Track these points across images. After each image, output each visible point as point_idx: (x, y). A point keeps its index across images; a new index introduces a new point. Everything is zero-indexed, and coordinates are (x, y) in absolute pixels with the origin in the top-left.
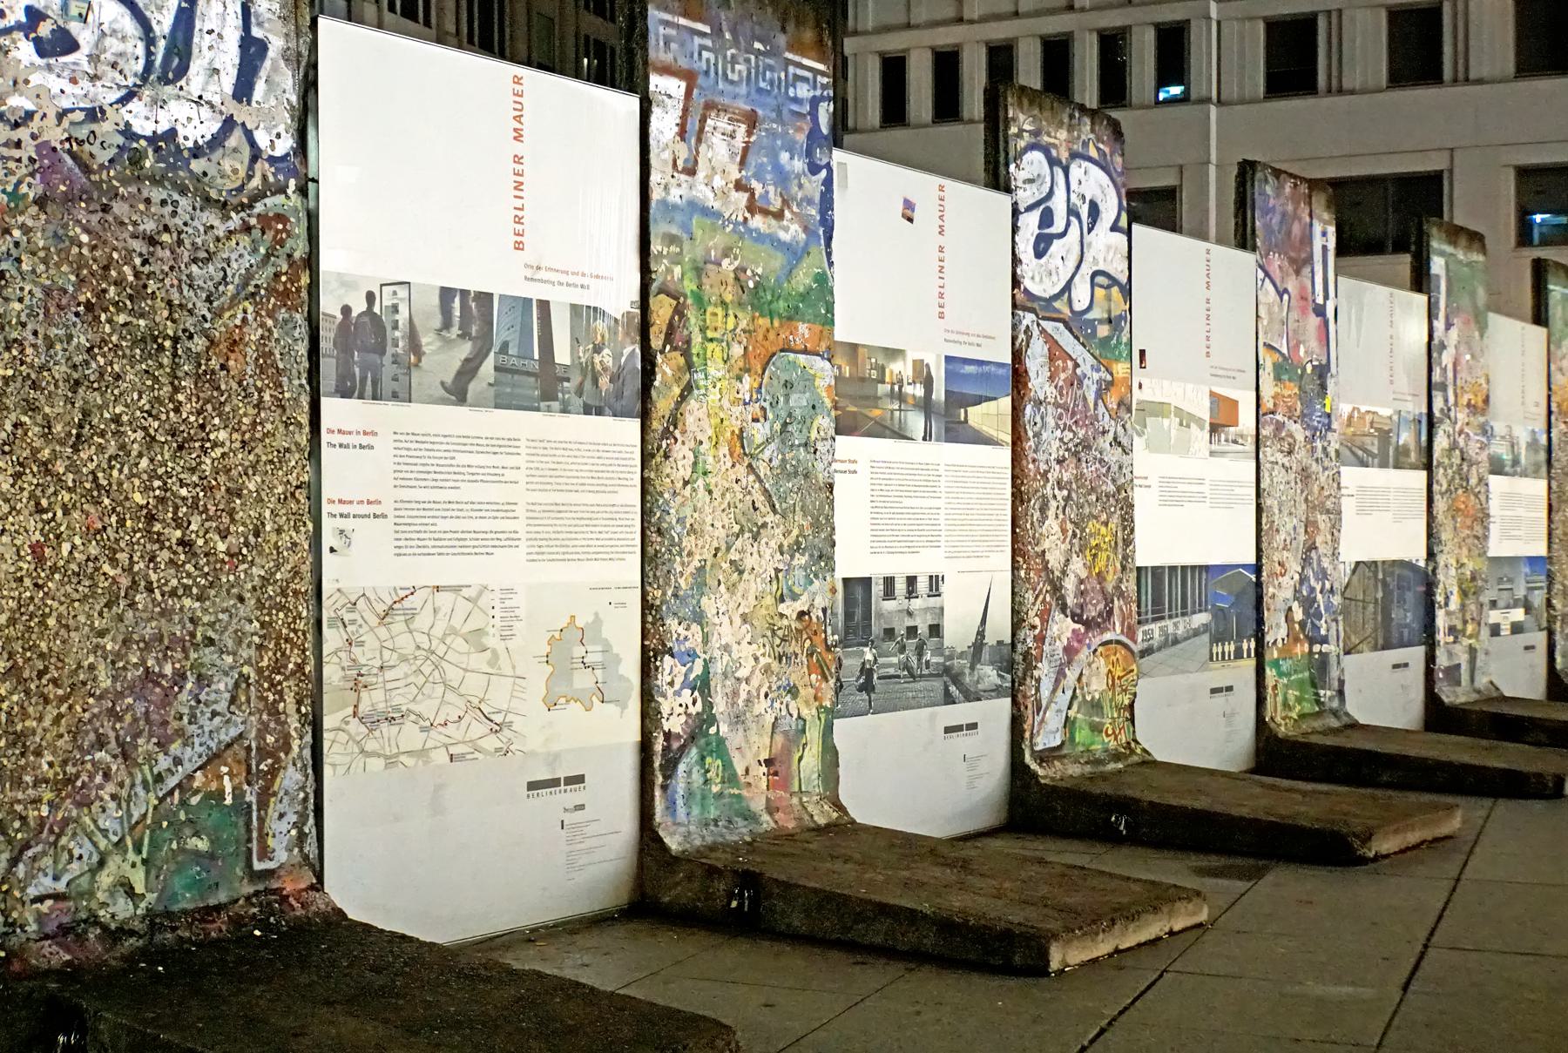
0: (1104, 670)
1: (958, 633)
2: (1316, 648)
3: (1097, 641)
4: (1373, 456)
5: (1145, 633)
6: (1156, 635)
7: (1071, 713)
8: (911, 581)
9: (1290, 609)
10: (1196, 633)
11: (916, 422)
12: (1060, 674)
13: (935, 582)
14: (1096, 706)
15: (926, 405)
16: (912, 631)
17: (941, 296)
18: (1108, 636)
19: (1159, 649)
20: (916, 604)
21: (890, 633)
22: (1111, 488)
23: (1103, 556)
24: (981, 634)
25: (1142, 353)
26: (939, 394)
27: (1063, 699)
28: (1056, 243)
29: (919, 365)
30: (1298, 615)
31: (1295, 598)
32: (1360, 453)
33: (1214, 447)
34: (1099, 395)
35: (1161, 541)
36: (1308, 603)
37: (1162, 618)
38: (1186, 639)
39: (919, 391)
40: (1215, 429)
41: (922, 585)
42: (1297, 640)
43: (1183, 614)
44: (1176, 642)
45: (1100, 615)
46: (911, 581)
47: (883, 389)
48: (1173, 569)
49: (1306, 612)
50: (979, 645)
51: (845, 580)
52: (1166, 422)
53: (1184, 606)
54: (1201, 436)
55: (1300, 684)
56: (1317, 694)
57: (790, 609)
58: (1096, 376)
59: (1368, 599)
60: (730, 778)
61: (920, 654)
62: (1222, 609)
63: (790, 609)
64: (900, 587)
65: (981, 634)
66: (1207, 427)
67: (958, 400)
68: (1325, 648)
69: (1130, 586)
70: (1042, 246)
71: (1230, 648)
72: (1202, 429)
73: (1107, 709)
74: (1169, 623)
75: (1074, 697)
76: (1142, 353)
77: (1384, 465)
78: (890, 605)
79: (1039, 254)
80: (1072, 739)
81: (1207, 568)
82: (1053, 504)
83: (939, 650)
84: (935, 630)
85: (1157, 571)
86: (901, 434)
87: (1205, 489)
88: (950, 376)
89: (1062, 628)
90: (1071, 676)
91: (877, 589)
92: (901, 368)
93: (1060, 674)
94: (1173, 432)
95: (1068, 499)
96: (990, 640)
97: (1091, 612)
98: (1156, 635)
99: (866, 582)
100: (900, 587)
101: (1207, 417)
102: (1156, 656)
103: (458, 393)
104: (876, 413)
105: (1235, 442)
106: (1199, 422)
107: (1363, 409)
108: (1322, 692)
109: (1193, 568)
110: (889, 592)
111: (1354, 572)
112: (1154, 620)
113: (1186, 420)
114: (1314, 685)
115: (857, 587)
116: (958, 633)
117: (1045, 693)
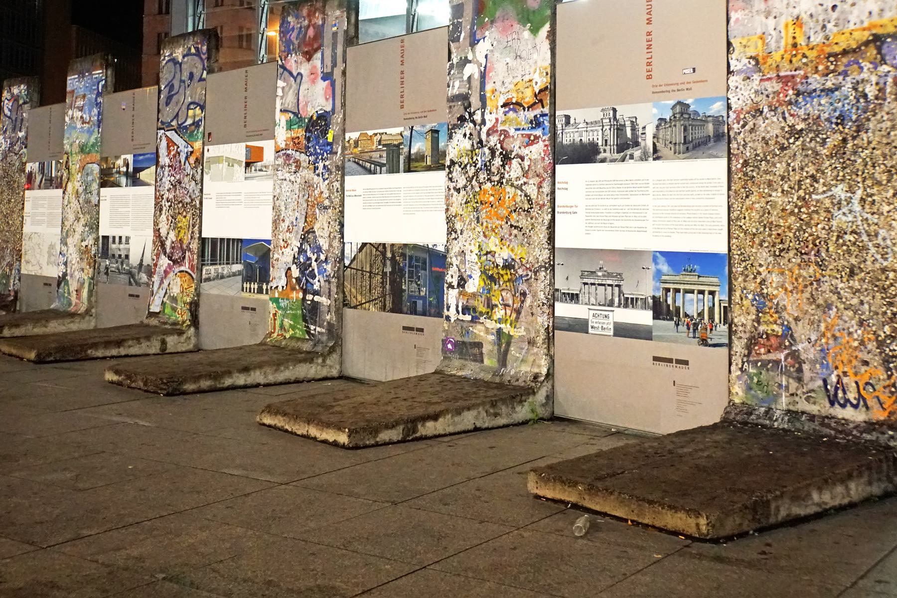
0: (179, 284)
1: (134, 260)
2: (309, 297)
3: (177, 270)
4: (381, 165)
5: (207, 270)
6: (213, 272)
7: (165, 300)
8: (120, 238)
9: (289, 269)
10: (234, 275)
11: (123, 180)
12: (162, 282)
13: (128, 239)
14: (174, 299)
15: (127, 174)
16: (120, 256)
17: (402, 97)
18: (182, 268)
19: (214, 279)
20: (122, 246)
21: (114, 255)
22: (189, 200)
23: (182, 231)
24: (142, 260)
25: (210, 134)
26: (131, 169)
27: (162, 293)
28: (175, 97)
29: (125, 160)
30: (296, 272)
31: (294, 263)
32: (368, 165)
33: (248, 175)
34: (187, 158)
35: (215, 226)
36: (304, 267)
37: (216, 264)
38: (229, 276)
39: (124, 169)
40: (248, 165)
41: (124, 240)
42: (293, 289)
43: (228, 264)
44: (222, 277)
45: (180, 258)
46: (120, 238)
47: (114, 170)
48: (222, 240)
49: (302, 272)
50: (141, 264)
51: (104, 237)
52: (221, 165)
53: (228, 259)
54: (240, 170)
55: (294, 317)
56: (308, 327)
57: (84, 244)
58: (186, 150)
59: (375, 271)
60: (69, 293)
61: (122, 264)
62: (250, 264)
63: (84, 244)
64: (117, 240)
65: (142, 260)
66: (244, 164)
67: (137, 170)
68: (317, 298)
69: (195, 246)
70: (169, 98)
71: (255, 286)
72: (240, 166)
73: (179, 302)
74: (219, 267)
75: (166, 293)
76: (210, 134)
77: (393, 170)
78: (114, 246)
79: (167, 104)
80: (164, 311)
81: (241, 240)
82: (164, 208)
83: (128, 265)
84: (127, 257)
85: (214, 241)
86: (119, 186)
87: (242, 198)
88: (134, 161)
89: (164, 262)
90: (166, 282)
91: (111, 240)
92: (120, 162)
93: (162, 282)
94: (224, 170)
95: (170, 206)
96: (145, 263)
97: (176, 257)
98: (213, 272)
99: (108, 237)
100: (117, 240)
101: (244, 160)
102: (211, 283)
103: (40, 187)
104: (112, 179)
105: (261, 170)
106: (239, 163)
107: (370, 133)
108: (312, 327)
109: (233, 240)
110: (114, 242)
111: (361, 250)
112: (212, 264)
113: (231, 162)
114: (305, 320)
115: (105, 238)
116: (134, 260)
117: (155, 288)
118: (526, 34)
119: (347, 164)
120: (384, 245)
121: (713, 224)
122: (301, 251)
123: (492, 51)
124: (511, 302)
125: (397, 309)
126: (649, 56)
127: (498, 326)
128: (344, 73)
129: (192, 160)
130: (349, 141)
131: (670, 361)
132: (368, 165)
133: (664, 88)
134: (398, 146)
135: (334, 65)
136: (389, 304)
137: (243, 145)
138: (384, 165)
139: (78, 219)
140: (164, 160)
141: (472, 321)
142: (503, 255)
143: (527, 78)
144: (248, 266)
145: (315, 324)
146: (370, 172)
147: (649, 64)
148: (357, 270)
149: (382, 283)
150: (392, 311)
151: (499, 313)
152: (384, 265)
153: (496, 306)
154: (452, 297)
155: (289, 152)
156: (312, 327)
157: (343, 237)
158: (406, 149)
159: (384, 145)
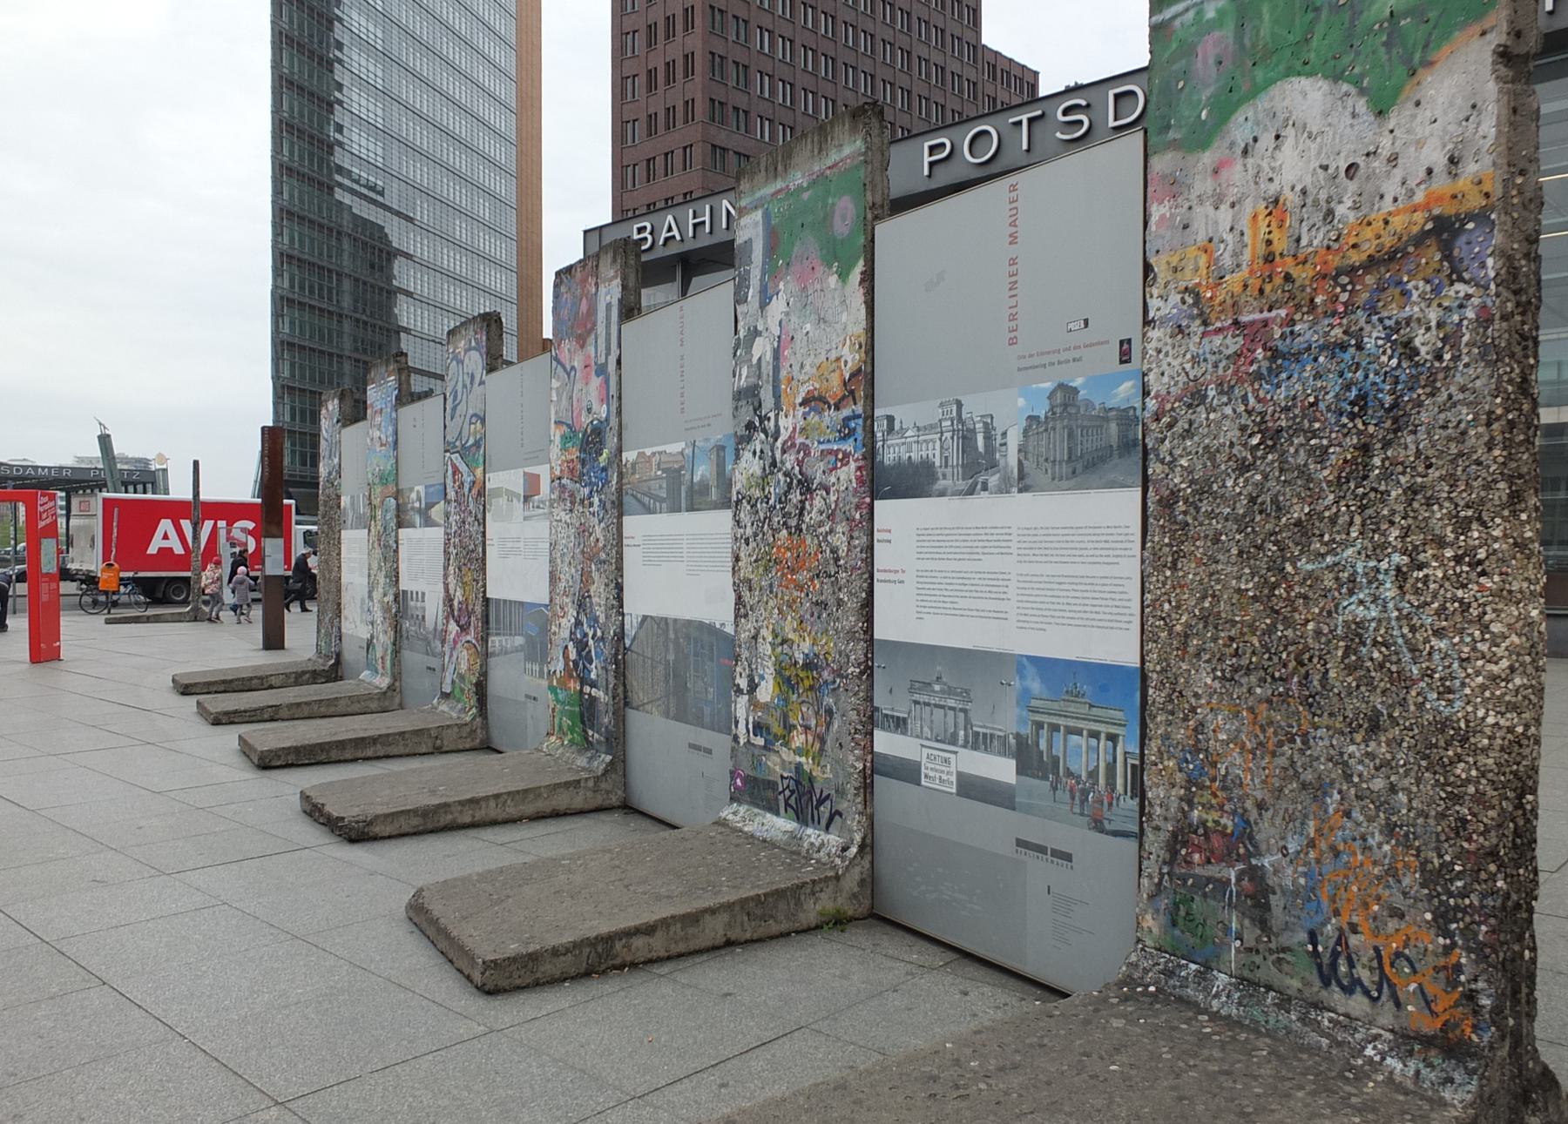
2: (587, 689)
4: (662, 500)
11: (417, 519)
14: (462, 677)
32: (646, 500)
36: (581, 645)
40: (526, 499)
42: (571, 676)
49: (579, 653)
54: (518, 505)
71: (536, 668)
77: (675, 509)
81: (521, 604)
85: (497, 601)
89: (453, 628)
107: (648, 452)
114: (583, 722)
118: (833, 280)
121: (1115, 610)
122: (578, 623)
123: (787, 314)
124: (813, 723)
126: (1012, 302)
127: (798, 759)
129: (474, 491)
131: (1041, 849)
132: (646, 500)
133: (1037, 361)
134: (678, 471)
135: (608, 354)
137: (520, 471)
139: (380, 568)
140: (451, 495)
141: (765, 747)
142: (803, 649)
143: (833, 355)
144: (529, 639)
147: (1013, 318)
150: (677, 718)
151: (798, 740)
152: (667, 650)
153: (794, 727)
154: (741, 706)
155: (564, 481)
157: (622, 606)
158: (688, 477)
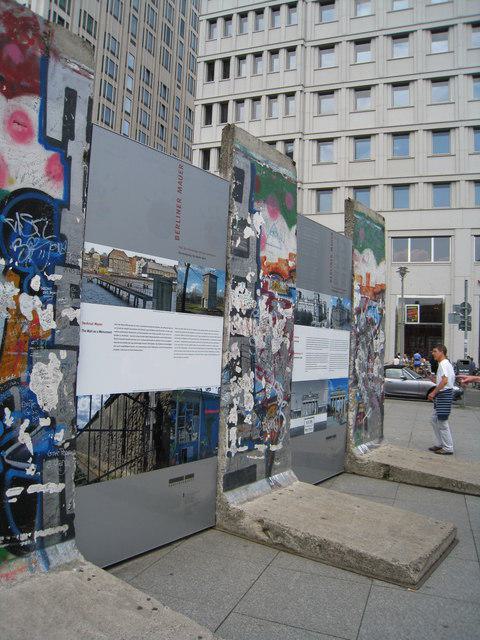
4: (146, 298)
68: (32, 489)
107: (130, 254)
119: (86, 287)
120: (146, 395)
125: (162, 461)
128: (87, 157)
130: (91, 254)
134: (170, 281)
136: (151, 461)
138: (150, 299)
145: (30, 528)
146: (127, 303)
148: (100, 431)
149: (143, 440)
150: (156, 468)
152: (146, 417)
156: (24, 536)
158: (180, 287)
159: (150, 275)
